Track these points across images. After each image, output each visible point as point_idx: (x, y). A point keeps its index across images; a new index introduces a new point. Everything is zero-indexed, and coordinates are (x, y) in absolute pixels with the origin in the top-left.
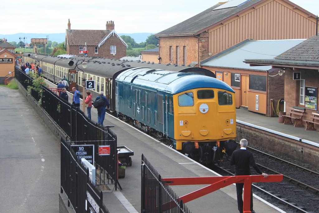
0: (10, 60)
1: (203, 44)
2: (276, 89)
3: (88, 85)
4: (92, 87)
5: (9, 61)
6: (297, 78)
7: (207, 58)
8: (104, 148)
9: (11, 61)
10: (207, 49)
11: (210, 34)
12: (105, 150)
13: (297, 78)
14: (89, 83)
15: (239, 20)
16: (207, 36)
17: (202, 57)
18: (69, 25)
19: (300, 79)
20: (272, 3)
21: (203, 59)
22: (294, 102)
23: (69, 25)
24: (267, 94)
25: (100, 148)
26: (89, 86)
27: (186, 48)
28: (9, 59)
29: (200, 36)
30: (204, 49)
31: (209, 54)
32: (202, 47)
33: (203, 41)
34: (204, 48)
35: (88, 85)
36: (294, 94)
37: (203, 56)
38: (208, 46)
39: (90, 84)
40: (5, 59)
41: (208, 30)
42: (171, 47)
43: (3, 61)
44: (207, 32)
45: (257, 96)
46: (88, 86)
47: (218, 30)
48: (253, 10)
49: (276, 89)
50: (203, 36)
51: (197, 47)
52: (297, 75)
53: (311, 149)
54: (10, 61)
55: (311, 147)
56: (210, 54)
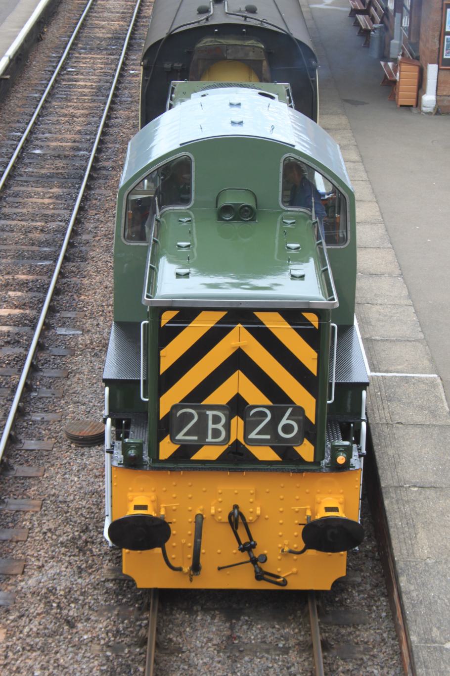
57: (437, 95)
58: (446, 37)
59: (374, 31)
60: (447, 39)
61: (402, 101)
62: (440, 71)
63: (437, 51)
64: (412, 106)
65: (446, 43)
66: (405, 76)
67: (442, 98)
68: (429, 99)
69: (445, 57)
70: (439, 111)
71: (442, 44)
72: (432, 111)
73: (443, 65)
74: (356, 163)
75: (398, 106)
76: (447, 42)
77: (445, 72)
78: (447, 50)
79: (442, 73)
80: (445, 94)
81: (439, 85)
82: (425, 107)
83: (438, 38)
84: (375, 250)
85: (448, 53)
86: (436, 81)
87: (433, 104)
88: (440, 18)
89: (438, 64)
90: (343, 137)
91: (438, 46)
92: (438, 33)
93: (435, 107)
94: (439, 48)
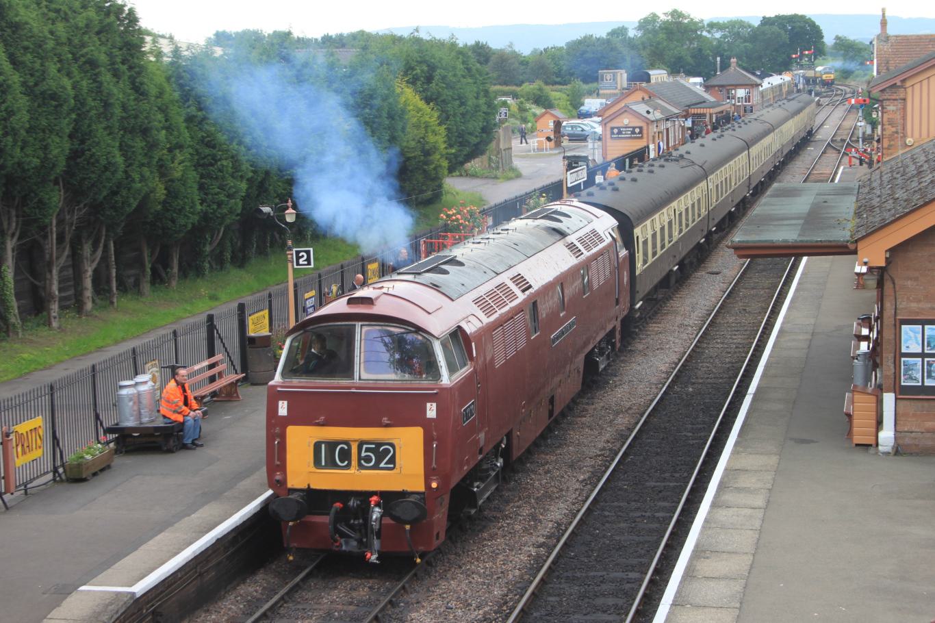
0: (637, 130)
1: (890, 117)
3: (298, 258)
4: (306, 263)
5: (633, 132)
9: (639, 133)
10: (900, 128)
11: (909, 91)
14: (301, 255)
16: (902, 96)
18: (884, 23)
21: (891, 154)
23: (884, 23)
26: (301, 261)
28: (634, 128)
30: (894, 129)
31: (907, 142)
32: (889, 125)
33: (891, 108)
34: (893, 127)
35: (298, 258)
37: (889, 146)
38: (904, 118)
39: (303, 256)
40: (624, 129)
41: (903, 81)
43: (620, 133)
44: (901, 87)
50: (889, 97)
54: (635, 133)
57: (895, 430)
58: (903, 359)
59: (857, 359)
60: (904, 362)
61: (858, 439)
62: (898, 401)
63: (892, 377)
64: (871, 445)
65: (902, 367)
66: (860, 406)
67: (903, 434)
68: (887, 436)
69: (903, 384)
70: (899, 450)
71: (897, 368)
72: (890, 451)
73: (900, 394)
74: (757, 510)
75: (854, 445)
76: (904, 365)
77: (905, 402)
78: (904, 375)
79: (901, 403)
80: (906, 429)
81: (898, 418)
82: (881, 445)
83: (893, 360)
84: (715, 610)
85: (906, 379)
86: (894, 413)
87: (891, 442)
88: (893, 336)
89: (895, 392)
90: (759, 480)
91: (893, 371)
92: (892, 355)
93: (894, 446)
94: (895, 373)
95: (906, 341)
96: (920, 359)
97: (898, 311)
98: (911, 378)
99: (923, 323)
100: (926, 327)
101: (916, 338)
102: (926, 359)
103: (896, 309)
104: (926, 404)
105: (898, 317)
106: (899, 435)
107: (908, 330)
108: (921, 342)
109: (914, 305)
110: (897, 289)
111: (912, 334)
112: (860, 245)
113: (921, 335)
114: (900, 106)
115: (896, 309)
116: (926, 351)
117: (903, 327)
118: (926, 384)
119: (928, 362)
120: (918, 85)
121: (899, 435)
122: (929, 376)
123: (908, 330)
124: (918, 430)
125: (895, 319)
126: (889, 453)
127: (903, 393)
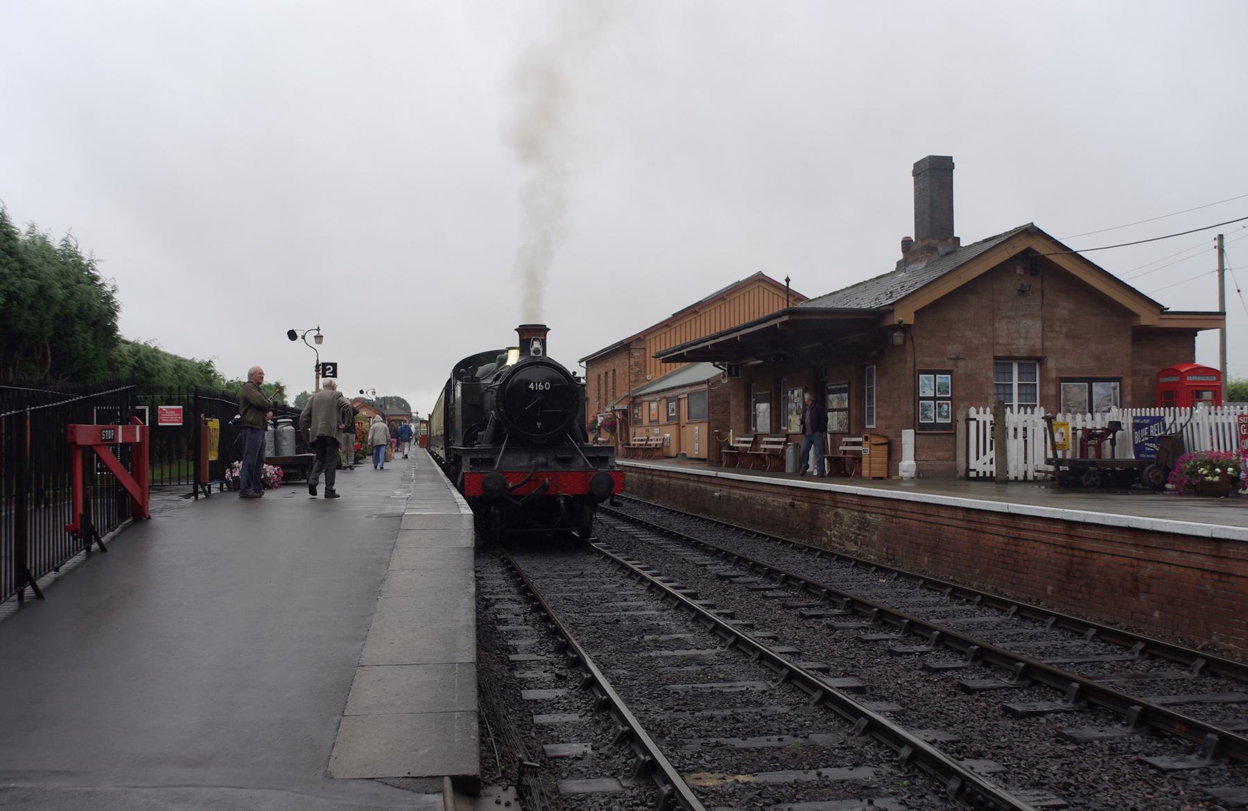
2: (723, 412)
4: (332, 374)
6: (734, 374)
7: (643, 384)
8: (168, 410)
12: (172, 412)
13: (734, 374)
14: (327, 367)
15: (698, 319)
17: (635, 381)
19: (738, 376)
20: (756, 290)
22: (742, 426)
24: (709, 423)
25: (161, 409)
26: (327, 373)
27: (617, 371)
29: (631, 347)
30: (638, 369)
31: (647, 378)
33: (636, 354)
36: (742, 413)
39: (329, 369)
42: (599, 376)
44: (643, 340)
45: (697, 428)
46: (325, 373)
47: (663, 336)
48: (724, 302)
49: (723, 412)
51: (628, 367)
52: (733, 368)
53: (732, 487)
55: (730, 483)
56: (648, 377)
57: (915, 460)
58: (921, 402)
63: (912, 416)
65: (920, 408)
67: (921, 462)
69: (921, 422)
73: (919, 430)
79: (918, 437)
80: (923, 459)
83: (912, 403)
86: (913, 446)
91: (913, 411)
92: (912, 399)
94: (915, 413)
95: (922, 389)
96: (933, 402)
97: (916, 364)
98: (926, 417)
99: (935, 372)
100: (937, 376)
101: (930, 384)
102: (937, 402)
103: (915, 362)
104: (937, 438)
105: (917, 368)
106: (918, 463)
107: (924, 378)
108: (933, 388)
109: (927, 359)
110: (916, 346)
111: (927, 382)
112: (896, 308)
113: (933, 382)
114: (642, 353)
115: (915, 362)
116: (937, 396)
117: (920, 376)
118: (937, 422)
119: (939, 403)
120: (684, 325)
121: (918, 463)
122: (940, 415)
123: (924, 378)
124: (931, 459)
125: (914, 371)
126: (912, 478)
127: (922, 430)
